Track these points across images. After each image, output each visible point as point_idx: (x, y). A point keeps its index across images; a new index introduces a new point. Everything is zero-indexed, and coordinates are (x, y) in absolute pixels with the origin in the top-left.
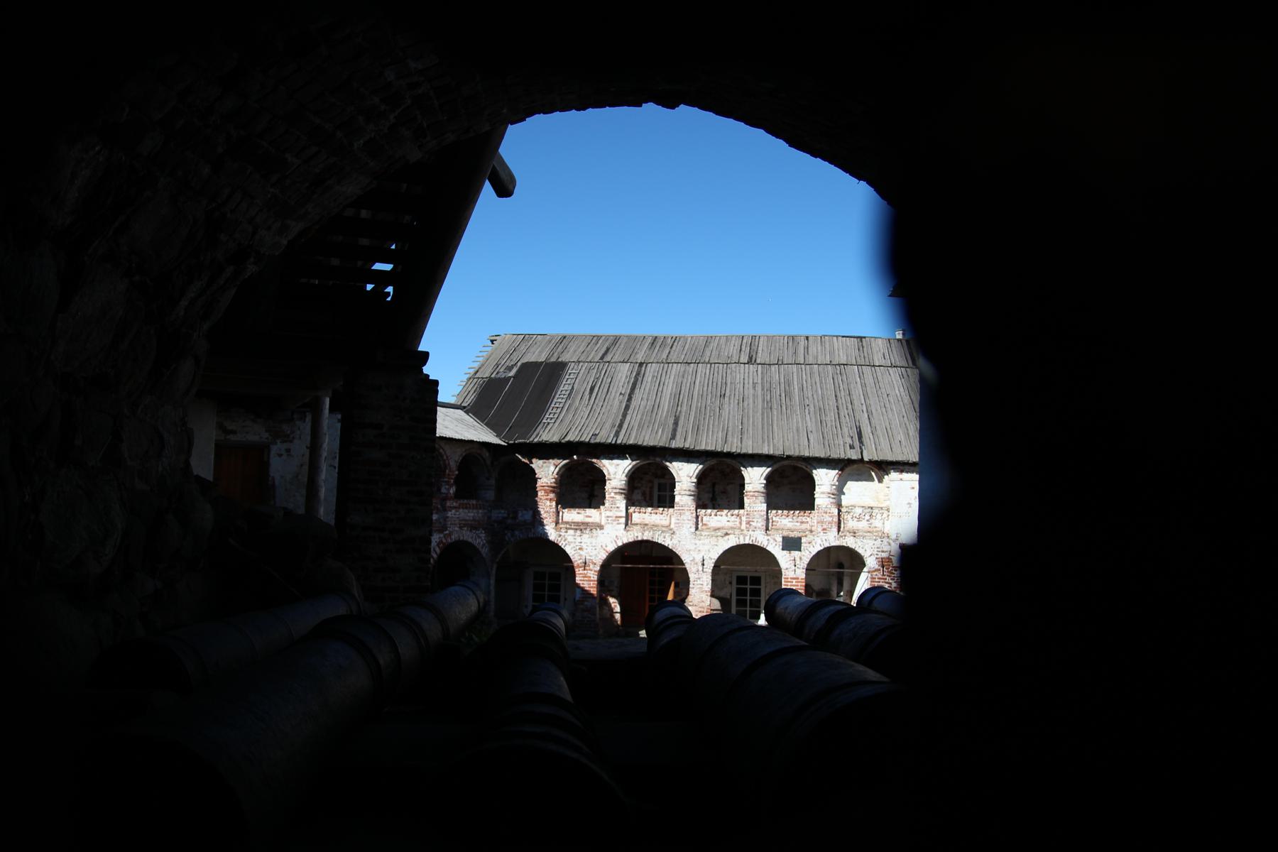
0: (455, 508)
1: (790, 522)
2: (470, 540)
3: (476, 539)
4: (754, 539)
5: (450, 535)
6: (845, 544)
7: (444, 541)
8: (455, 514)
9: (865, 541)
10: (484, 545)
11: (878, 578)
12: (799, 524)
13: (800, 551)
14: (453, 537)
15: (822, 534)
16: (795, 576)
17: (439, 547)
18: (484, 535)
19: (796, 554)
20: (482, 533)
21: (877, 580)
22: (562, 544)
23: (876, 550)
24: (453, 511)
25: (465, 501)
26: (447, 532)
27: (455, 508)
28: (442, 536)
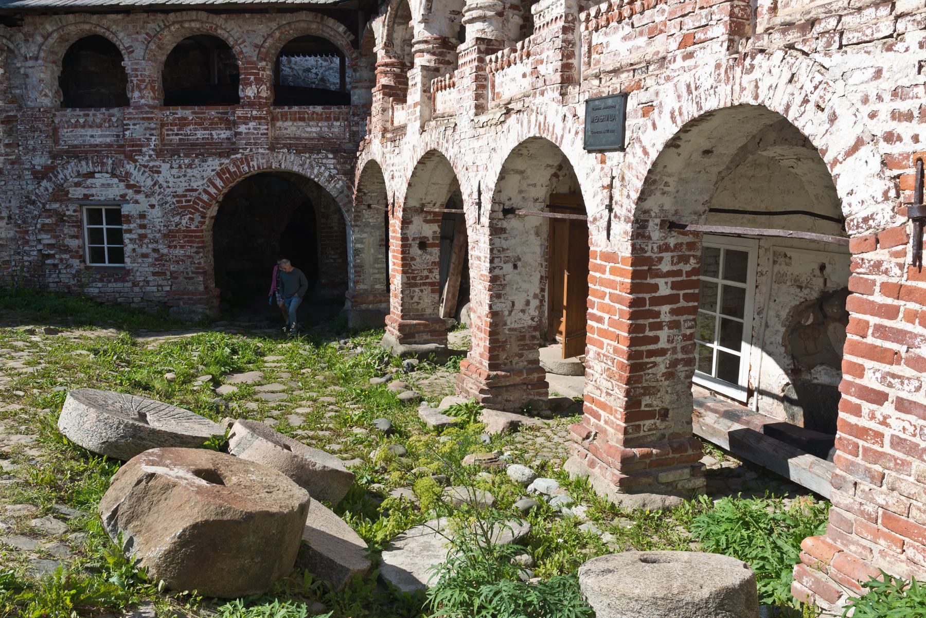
0: (255, 118)
1: (625, 38)
2: (296, 169)
3: (312, 167)
4: (541, 118)
5: (246, 160)
6: (748, 99)
7: (233, 169)
8: (255, 129)
9: (836, 60)
10: (332, 177)
11: (887, 289)
12: (642, 41)
13: (623, 149)
14: (254, 163)
15: (679, 62)
16: (609, 249)
17: (221, 178)
18: (333, 161)
19: (614, 157)
20: (327, 158)
21: (878, 298)
22: (383, 167)
23: (885, 109)
24: (252, 124)
25: (286, 109)
26: (239, 156)
27: (255, 118)
28: (227, 161)
